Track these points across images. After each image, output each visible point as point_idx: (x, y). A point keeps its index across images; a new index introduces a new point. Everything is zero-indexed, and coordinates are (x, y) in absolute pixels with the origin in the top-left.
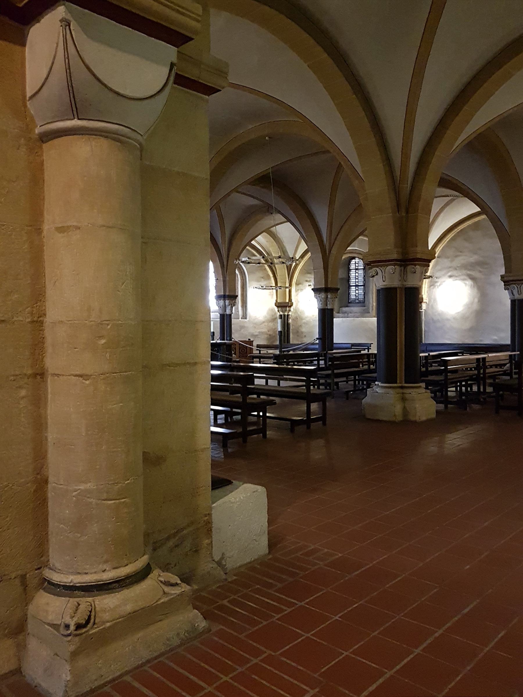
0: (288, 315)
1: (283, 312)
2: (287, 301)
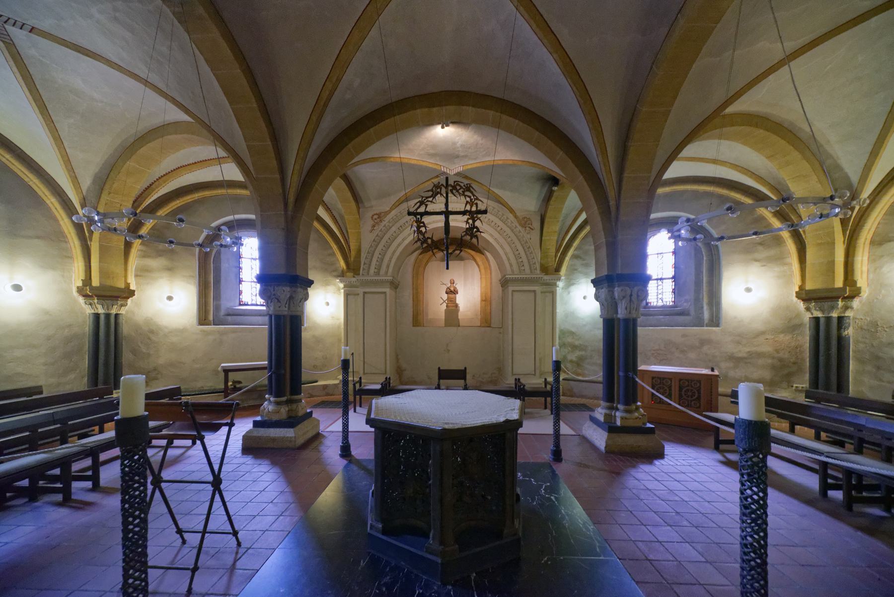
0: (840, 319)
1: (823, 311)
2: (839, 283)
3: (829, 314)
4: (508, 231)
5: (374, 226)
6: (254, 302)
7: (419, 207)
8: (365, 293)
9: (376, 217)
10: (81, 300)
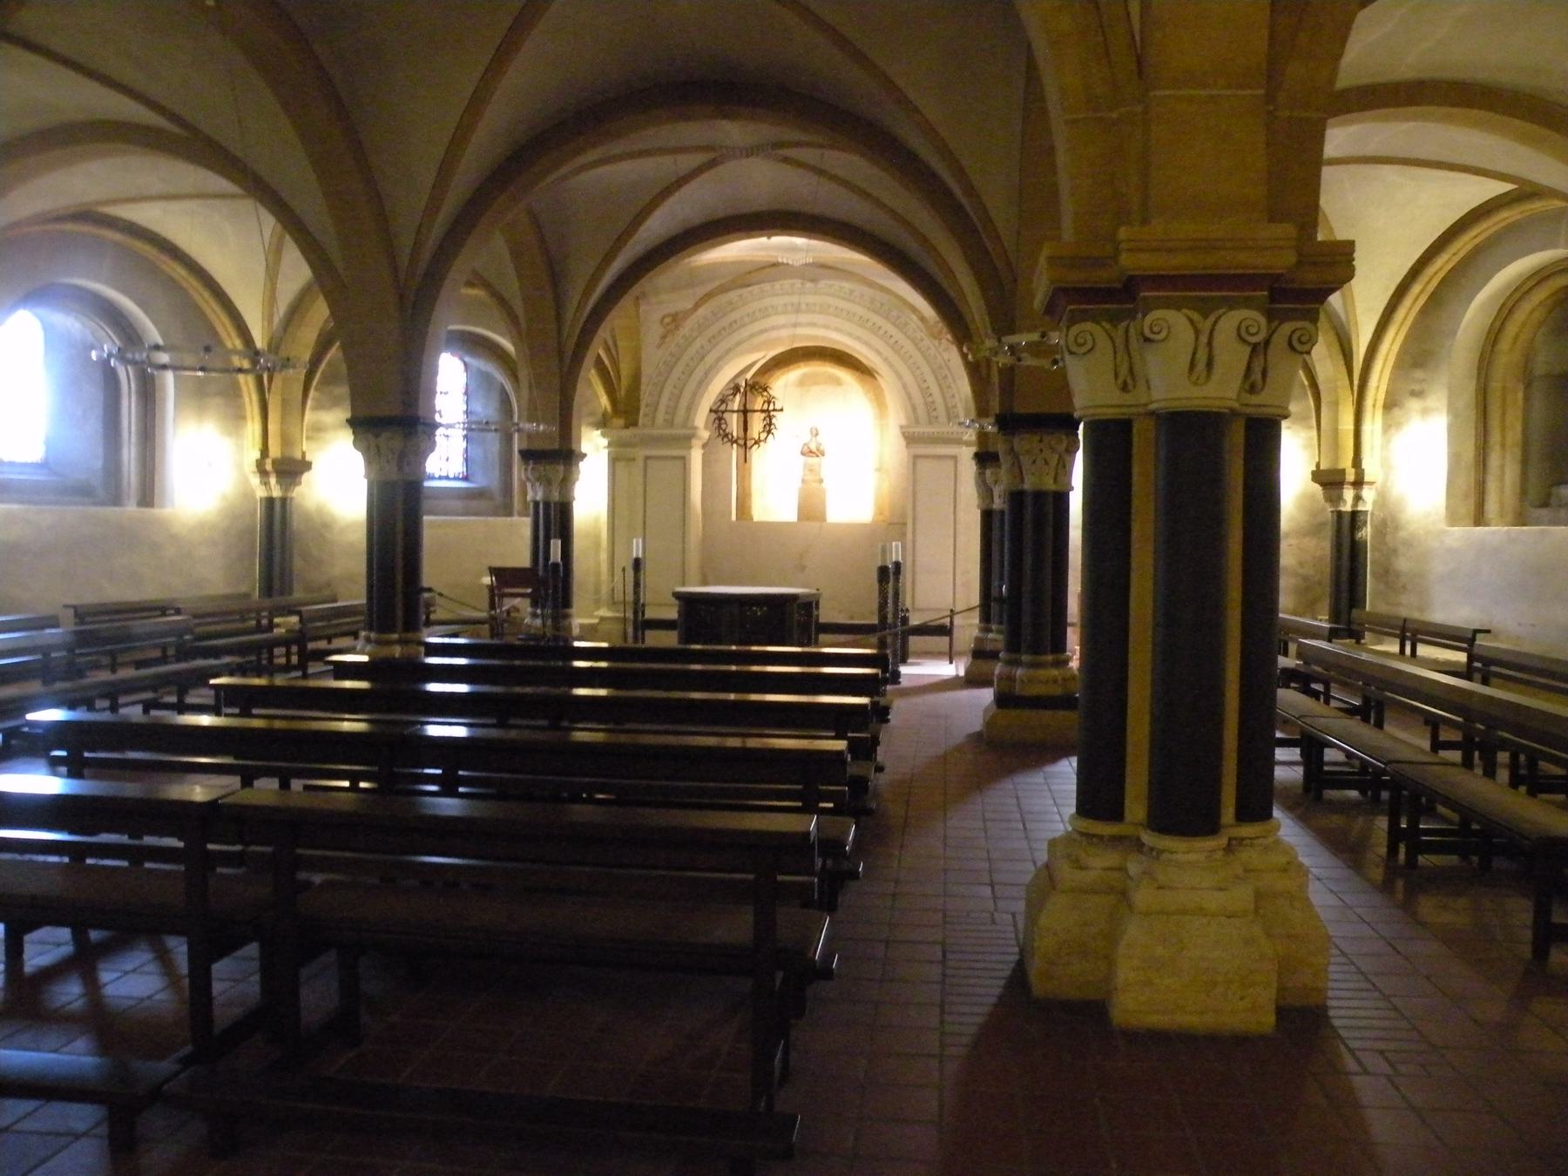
0: (1354, 514)
3: (1337, 507)
4: (909, 346)
5: (664, 337)
6: (444, 474)
7: (720, 406)
8: (647, 458)
9: (667, 320)
10: (255, 480)
